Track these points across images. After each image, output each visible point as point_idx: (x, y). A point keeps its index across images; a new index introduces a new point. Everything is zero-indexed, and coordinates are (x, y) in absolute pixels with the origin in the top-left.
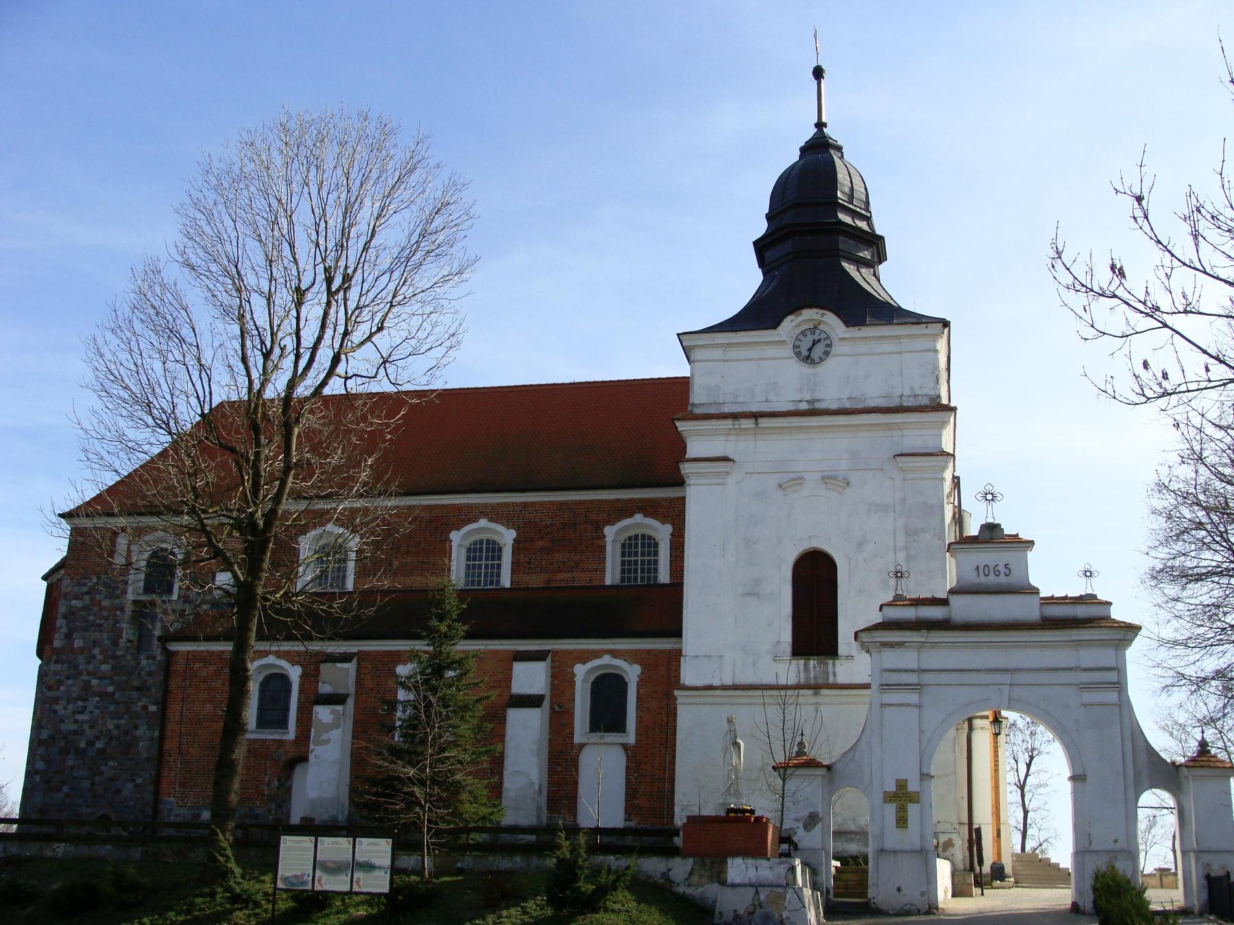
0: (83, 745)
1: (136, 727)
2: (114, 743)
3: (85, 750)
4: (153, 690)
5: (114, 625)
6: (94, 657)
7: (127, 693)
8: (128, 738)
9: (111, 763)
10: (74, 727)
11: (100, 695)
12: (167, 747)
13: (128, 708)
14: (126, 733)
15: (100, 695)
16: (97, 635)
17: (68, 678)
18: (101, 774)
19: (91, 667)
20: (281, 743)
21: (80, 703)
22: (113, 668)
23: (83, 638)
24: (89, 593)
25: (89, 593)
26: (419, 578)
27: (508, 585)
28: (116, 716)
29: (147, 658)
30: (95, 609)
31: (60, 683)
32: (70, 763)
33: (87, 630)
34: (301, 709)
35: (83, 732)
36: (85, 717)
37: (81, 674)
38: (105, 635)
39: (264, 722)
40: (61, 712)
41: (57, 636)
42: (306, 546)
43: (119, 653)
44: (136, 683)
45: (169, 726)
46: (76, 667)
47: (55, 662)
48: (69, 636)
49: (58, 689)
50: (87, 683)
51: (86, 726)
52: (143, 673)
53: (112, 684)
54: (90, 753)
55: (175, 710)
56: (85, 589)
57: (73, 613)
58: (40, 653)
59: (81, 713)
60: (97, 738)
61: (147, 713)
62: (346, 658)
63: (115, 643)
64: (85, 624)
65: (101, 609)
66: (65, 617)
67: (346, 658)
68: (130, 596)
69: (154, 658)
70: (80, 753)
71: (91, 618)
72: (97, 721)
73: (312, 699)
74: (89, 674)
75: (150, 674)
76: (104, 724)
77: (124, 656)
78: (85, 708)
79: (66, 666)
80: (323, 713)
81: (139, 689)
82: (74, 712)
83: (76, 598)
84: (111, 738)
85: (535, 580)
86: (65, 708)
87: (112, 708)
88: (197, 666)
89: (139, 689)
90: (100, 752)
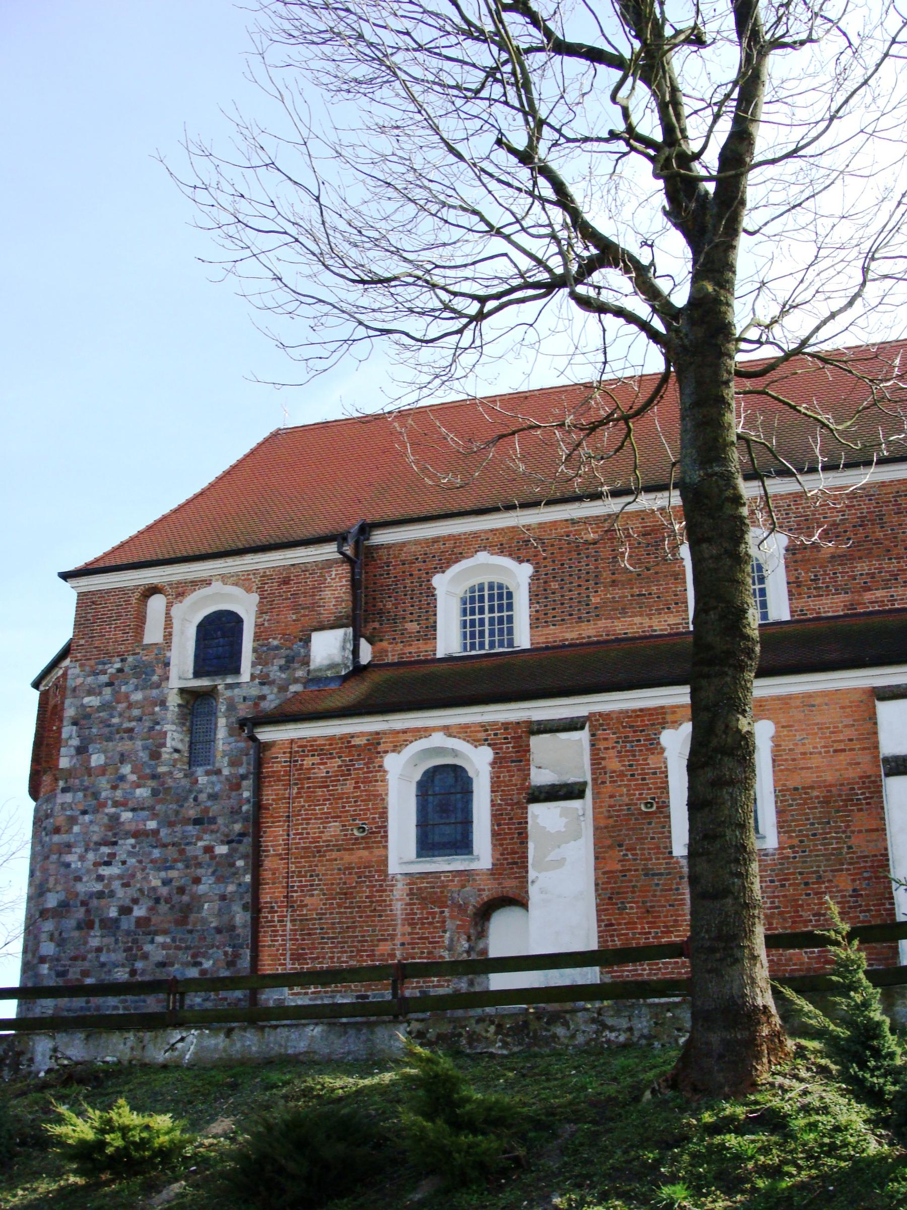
0: (113, 913)
1: (197, 881)
2: (163, 908)
3: (116, 921)
4: (220, 821)
5: (152, 729)
6: (122, 778)
7: (178, 828)
8: (186, 898)
9: (160, 939)
10: (99, 887)
11: (136, 835)
12: (265, 898)
13: (182, 852)
14: (181, 890)
15: (136, 835)
16: (125, 746)
17: (84, 812)
18: (145, 957)
19: (119, 794)
20: (466, 876)
21: (105, 850)
22: (155, 793)
23: (105, 752)
24: (110, 684)
25: (110, 684)
26: (637, 620)
27: (786, 617)
28: (164, 865)
29: (208, 773)
30: (121, 707)
31: (73, 820)
32: (94, 942)
33: (109, 739)
34: (497, 817)
35: (112, 894)
36: (114, 870)
37: (104, 805)
38: (139, 744)
39: (427, 845)
40: (76, 865)
41: (63, 750)
42: (449, 589)
43: (162, 769)
44: (192, 813)
45: (268, 863)
46: (96, 795)
47: (64, 790)
48: (82, 750)
49: (69, 831)
50: (115, 818)
51: (116, 885)
52: (203, 797)
53: (154, 816)
54: (127, 924)
55: (275, 836)
56: (104, 679)
57: (87, 716)
58: (34, 791)
59: (108, 864)
60: (135, 901)
61: (213, 857)
62: (573, 725)
63: (155, 755)
64: (106, 730)
65: (130, 706)
66: (75, 723)
67: (573, 725)
68: (176, 681)
69: (218, 772)
70: (109, 926)
71: (115, 720)
72: (133, 876)
73: (519, 794)
74: (116, 804)
75: (213, 797)
76: (145, 879)
77: (171, 773)
78: (113, 855)
79: (80, 795)
80: (543, 816)
81: (197, 822)
82: (96, 864)
83: (90, 692)
84: (157, 900)
85: (831, 605)
86: (82, 858)
87: (156, 853)
88: (308, 762)
89: (197, 822)
90: (142, 922)
